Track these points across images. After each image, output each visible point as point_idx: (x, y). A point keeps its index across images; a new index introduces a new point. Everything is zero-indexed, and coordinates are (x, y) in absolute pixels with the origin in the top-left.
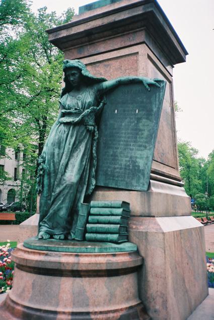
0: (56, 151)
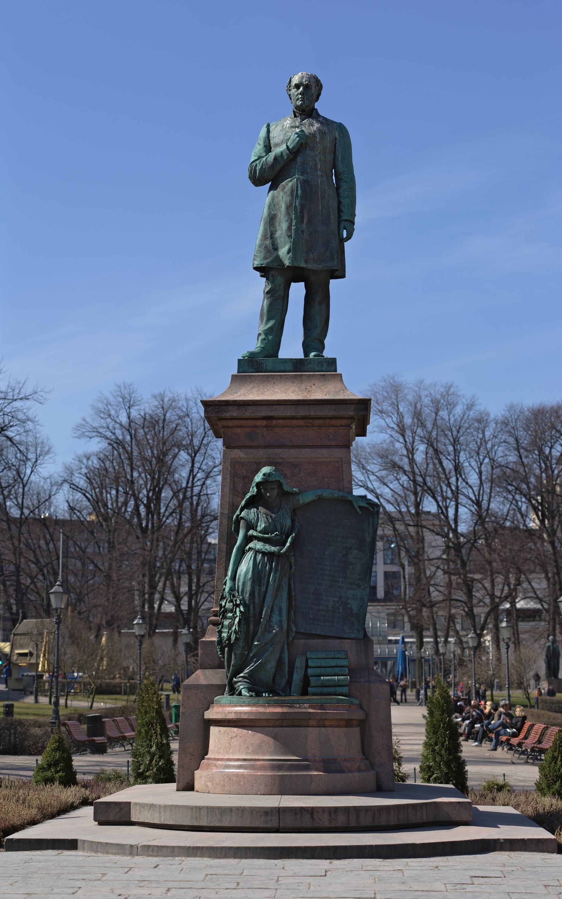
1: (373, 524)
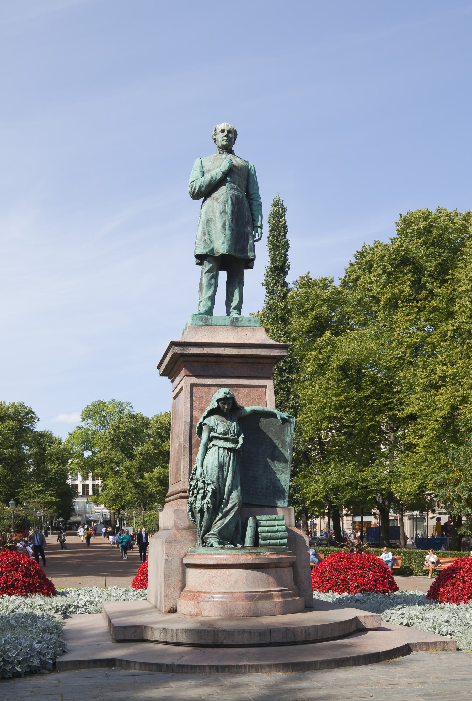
1: (291, 431)
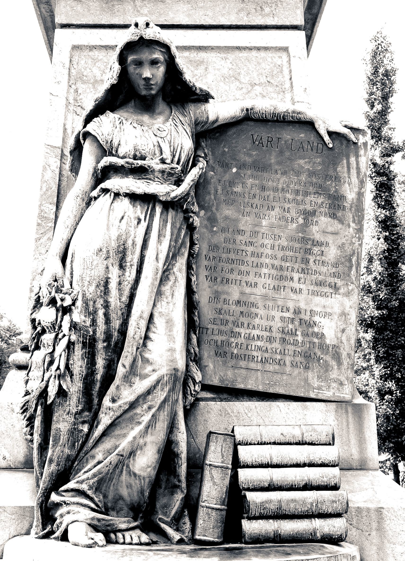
0: (114, 273)
1: (358, 168)
